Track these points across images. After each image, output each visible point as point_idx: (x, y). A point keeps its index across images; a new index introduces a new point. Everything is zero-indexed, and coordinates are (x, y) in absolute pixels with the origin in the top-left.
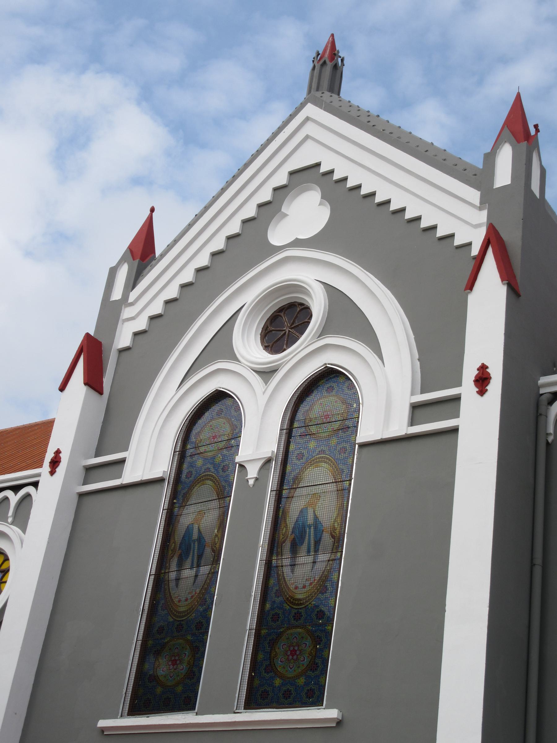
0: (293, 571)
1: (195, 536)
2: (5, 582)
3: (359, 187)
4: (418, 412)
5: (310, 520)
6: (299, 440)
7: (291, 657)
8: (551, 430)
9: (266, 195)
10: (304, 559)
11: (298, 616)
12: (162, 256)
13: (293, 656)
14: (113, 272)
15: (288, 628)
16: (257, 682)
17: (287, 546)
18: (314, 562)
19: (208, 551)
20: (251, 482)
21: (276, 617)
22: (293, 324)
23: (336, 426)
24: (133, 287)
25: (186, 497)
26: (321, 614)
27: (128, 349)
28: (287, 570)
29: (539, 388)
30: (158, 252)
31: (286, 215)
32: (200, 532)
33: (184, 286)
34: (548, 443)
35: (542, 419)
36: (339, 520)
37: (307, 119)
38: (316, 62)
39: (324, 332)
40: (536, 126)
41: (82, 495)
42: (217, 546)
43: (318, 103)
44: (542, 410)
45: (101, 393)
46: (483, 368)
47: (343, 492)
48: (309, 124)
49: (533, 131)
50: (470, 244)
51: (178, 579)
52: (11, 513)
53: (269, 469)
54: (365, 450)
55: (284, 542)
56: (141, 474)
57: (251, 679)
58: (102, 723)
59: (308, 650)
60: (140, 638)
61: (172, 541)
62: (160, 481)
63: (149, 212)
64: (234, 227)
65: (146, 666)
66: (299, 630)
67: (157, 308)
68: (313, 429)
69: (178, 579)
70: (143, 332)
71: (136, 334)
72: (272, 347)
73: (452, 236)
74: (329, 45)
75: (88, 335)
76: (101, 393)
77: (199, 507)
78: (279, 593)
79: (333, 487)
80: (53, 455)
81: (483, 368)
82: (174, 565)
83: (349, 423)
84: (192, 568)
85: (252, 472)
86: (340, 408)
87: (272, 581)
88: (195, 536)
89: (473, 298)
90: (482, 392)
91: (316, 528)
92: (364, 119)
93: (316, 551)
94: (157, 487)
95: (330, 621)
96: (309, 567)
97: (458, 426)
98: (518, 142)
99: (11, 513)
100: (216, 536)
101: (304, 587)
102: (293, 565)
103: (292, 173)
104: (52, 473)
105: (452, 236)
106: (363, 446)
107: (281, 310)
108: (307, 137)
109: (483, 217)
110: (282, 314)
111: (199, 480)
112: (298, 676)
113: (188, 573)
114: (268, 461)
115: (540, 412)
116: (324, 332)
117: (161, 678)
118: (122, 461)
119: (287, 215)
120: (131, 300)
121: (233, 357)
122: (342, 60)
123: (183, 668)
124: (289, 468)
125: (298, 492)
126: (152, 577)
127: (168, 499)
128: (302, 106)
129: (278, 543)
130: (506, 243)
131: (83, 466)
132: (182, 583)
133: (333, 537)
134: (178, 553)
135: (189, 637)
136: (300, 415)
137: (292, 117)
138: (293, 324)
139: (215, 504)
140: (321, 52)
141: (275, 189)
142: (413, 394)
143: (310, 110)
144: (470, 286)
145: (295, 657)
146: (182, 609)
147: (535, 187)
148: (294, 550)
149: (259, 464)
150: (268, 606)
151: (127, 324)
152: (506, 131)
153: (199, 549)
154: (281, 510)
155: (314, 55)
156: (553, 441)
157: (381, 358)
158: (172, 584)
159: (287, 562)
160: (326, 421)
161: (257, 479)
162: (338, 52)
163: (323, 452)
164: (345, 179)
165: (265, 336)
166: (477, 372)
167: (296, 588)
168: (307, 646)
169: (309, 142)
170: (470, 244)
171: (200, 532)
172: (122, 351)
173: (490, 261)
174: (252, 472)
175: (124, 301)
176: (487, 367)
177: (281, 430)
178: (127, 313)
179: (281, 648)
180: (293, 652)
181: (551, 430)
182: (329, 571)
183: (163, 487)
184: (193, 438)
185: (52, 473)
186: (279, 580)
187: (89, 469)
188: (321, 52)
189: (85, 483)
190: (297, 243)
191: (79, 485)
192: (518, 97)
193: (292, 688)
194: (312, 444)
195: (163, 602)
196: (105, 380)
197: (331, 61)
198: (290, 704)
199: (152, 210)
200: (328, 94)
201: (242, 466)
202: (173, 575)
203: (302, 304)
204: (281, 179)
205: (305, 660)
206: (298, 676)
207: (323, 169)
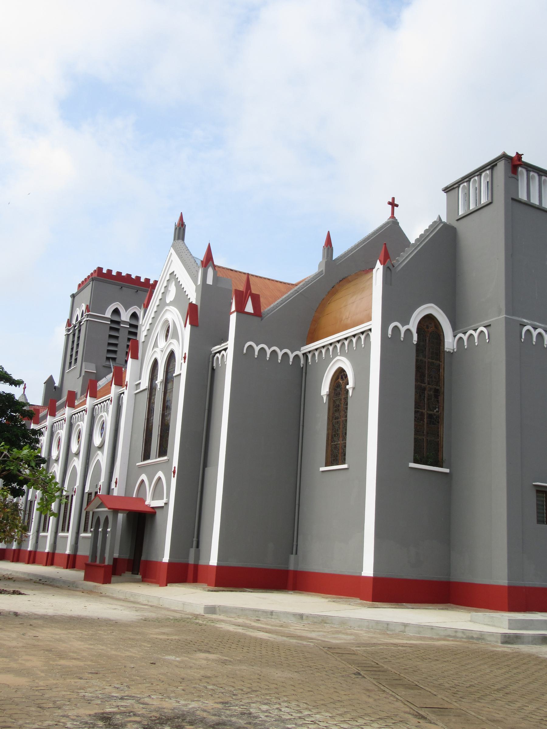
8: (215, 365)
9: (165, 284)
27: (144, 342)
29: (212, 352)
41: (136, 394)
54: (176, 377)
71: (146, 336)
114: (161, 382)
118: (140, 383)
151: (144, 332)
197: (178, 227)
200: (177, 241)
204: (168, 278)
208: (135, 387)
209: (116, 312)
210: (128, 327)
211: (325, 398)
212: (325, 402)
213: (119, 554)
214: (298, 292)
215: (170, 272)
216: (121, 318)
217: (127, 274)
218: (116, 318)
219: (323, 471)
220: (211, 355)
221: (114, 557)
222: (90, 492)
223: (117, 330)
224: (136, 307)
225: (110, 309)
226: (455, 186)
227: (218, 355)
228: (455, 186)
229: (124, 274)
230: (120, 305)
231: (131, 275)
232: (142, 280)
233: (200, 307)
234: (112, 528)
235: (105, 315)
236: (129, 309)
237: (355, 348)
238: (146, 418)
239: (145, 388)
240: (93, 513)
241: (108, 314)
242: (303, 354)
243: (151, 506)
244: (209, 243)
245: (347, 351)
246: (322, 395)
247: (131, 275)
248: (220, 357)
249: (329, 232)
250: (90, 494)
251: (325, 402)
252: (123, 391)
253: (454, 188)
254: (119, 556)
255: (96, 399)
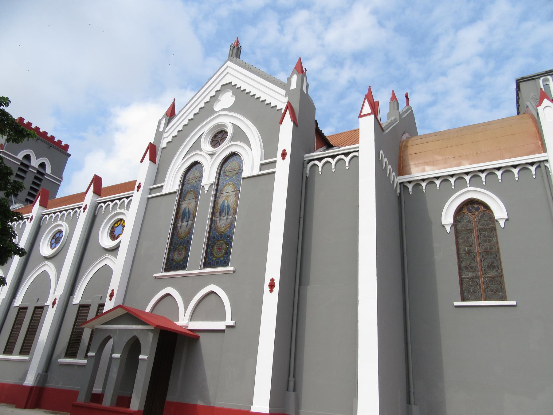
0: (220, 222)
1: (187, 211)
2: (124, 230)
3: (245, 90)
4: (263, 166)
5: (226, 204)
6: (222, 177)
7: (219, 251)
8: (308, 172)
9: (213, 93)
10: (224, 218)
11: (221, 237)
12: (177, 115)
13: (219, 250)
14: (160, 121)
15: (218, 241)
16: (207, 259)
17: (218, 214)
18: (227, 219)
19: (191, 216)
20: (206, 192)
21: (214, 238)
22: (222, 138)
23: (236, 172)
24: (167, 126)
25: (184, 197)
26: (229, 236)
27: (165, 148)
28: (218, 222)
30: (176, 114)
31: (220, 100)
32: (189, 210)
33: (184, 126)
34: (307, 177)
35: (305, 169)
36: (236, 204)
37: (228, 66)
38: (231, 47)
39: (231, 140)
40: (305, 69)
41: (149, 199)
42: (195, 214)
43: (231, 61)
44: (305, 166)
45: (155, 162)
46: (284, 150)
47: (237, 195)
48: (228, 68)
49: (304, 70)
50: (282, 109)
51: (181, 226)
52: (125, 206)
53: (212, 187)
54: (245, 180)
55: (217, 212)
56: (169, 190)
57: (205, 258)
58: (155, 275)
59: (224, 248)
60: (168, 246)
61: (179, 213)
62: (175, 192)
63: (173, 100)
64: (202, 105)
65: (170, 256)
66: (222, 241)
67: (175, 133)
68: (228, 174)
69: (181, 226)
70: (170, 142)
71: (168, 143)
72: (214, 146)
73: (276, 106)
74: (236, 41)
75: (150, 143)
76: (155, 162)
77: (189, 201)
78: (215, 229)
79: (234, 193)
80: (138, 185)
81: (284, 150)
82: (180, 221)
83: (240, 171)
84: (186, 222)
85: (206, 188)
86: (237, 166)
87: (213, 226)
88: (187, 211)
89: (282, 127)
90: (284, 159)
91: (228, 207)
92: (247, 66)
93: (228, 215)
94: (174, 195)
95: (232, 238)
96: (225, 220)
97: (275, 171)
98: (299, 74)
99: (125, 206)
100: (194, 211)
101: (224, 227)
102: (220, 220)
103: (222, 86)
104: (138, 191)
105: (276, 106)
106: (244, 178)
107: (218, 133)
108: (228, 73)
109: (286, 100)
110: (218, 135)
111: (188, 192)
112: (221, 257)
113: (185, 224)
114: (212, 185)
115: (304, 166)
116: (232, 140)
117: (175, 259)
118: (162, 186)
119: (220, 100)
120: (166, 131)
121: (200, 149)
122: (241, 47)
123: (183, 256)
124: (219, 187)
125: (222, 195)
126: (172, 225)
127: (178, 199)
128: (226, 62)
129: (215, 212)
130: (294, 110)
131: (149, 189)
132: (182, 227)
133: (234, 210)
134: (181, 217)
135: (185, 245)
136: (223, 169)
137: (222, 66)
138: (222, 138)
139: (194, 200)
140: (233, 44)
141: (216, 91)
142: (261, 160)
143: (229, 63)
144: (281, 123)
145: (220, 251)
146: (182, 236)
147: (305, 89)
148: (220, 215)
149: (209, 186)
150: (211, 234)
152: (295, 71)
153: (188, 215)
154: (216, 201)
155: (231, 44)
156: (308, 176)
157: (251, 148)
158: (179, 228)
159: (218, 219)
160: (232, 170)
161: (208, 191)
162: (239, 43)
163: (231, 181)
164: (240, 87)
165: (212, 142)
166: (282, 152)
167: (221, 227)
168: (224, 247)
169: (228, 74)
170: (282, 109)
171: (189, 210)
172: (163, 149)
173: (288, 114)
174: (206, 188)
175: (164, 131)
176: (286, 150)
177: (216, 174)
178: (165, 135)
179: (216, 247)
180: (220, 249)
181: (308, 172)
182: (232, 222)
183: (176, 195)
184: (187, 178)
185: (138, 191)
186: (215, 225)
187: (151, 190)
188: (233, 44)
189: (149, 195)
190: (224, 110)
191: (148, 195)
192: (300, 59)
193: (219, 261)
194: (227, 179)
195: (176, 234)
196: (157, 159)
198: (218, 266)
199: (174, 100)
200: (235, 58)
201: (203, 187)
202: (179, 225)
203: (225, 131)
204: (218, 88)
205: (223, 251)
206: (221, 257)
207: (233, 84)
208: (149, 191)
209: (28, 157)
210: (36, 172)
211: (448, 229)
212: (448, 231)
213: (103, 388)
214: (391, 126)
215: (224, 82)
216: (31, 163)
217: (44, 131)
218: (26, 162)
219: (456, 307)
220: (306, 162)
221: (93, 392)
222: (24, 305)
223: (25, 172)
224: (46, 159)
225: (26, 151)
226: (535, 77)
227: (316, 162)
228: (535, 77)
229: (41, 131)
230: (32, 153)
231: (47, 133)
232: (56, 140)
233: (300, 111)
234: (97, 353)
235: (17, 156)
236: (43, 157)
237: (500, 181)
238: (173, 224)
239: (174, 190)
240: (93, 331)
241: (20, 156)
242: (400, 183)
243: (189, 328)
244: (300, 58)
245: (484, 183)
246: (442, 224)
247: (47, 133)
248: (320, 164)
249: (393, 91)
250: (22, 309)
251: (448, 231)
252: (81, 206)
253: (533, 79)
254: (102, 390)
255: (45, 209)
